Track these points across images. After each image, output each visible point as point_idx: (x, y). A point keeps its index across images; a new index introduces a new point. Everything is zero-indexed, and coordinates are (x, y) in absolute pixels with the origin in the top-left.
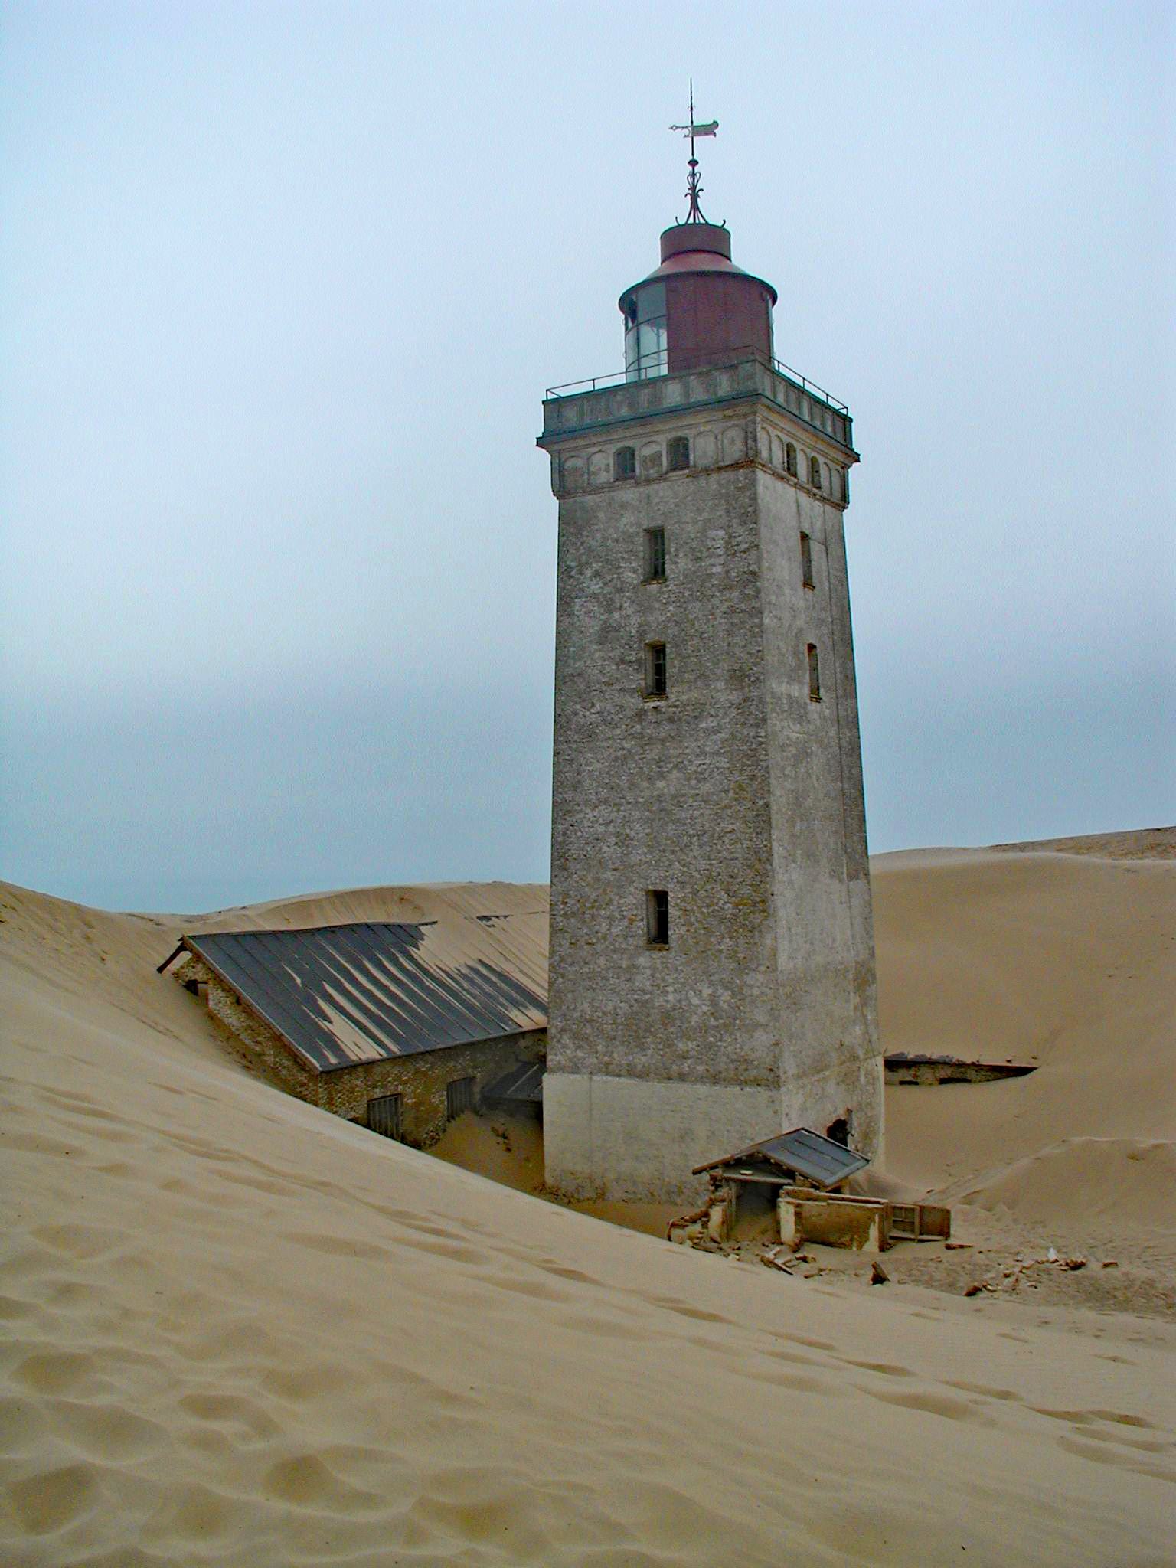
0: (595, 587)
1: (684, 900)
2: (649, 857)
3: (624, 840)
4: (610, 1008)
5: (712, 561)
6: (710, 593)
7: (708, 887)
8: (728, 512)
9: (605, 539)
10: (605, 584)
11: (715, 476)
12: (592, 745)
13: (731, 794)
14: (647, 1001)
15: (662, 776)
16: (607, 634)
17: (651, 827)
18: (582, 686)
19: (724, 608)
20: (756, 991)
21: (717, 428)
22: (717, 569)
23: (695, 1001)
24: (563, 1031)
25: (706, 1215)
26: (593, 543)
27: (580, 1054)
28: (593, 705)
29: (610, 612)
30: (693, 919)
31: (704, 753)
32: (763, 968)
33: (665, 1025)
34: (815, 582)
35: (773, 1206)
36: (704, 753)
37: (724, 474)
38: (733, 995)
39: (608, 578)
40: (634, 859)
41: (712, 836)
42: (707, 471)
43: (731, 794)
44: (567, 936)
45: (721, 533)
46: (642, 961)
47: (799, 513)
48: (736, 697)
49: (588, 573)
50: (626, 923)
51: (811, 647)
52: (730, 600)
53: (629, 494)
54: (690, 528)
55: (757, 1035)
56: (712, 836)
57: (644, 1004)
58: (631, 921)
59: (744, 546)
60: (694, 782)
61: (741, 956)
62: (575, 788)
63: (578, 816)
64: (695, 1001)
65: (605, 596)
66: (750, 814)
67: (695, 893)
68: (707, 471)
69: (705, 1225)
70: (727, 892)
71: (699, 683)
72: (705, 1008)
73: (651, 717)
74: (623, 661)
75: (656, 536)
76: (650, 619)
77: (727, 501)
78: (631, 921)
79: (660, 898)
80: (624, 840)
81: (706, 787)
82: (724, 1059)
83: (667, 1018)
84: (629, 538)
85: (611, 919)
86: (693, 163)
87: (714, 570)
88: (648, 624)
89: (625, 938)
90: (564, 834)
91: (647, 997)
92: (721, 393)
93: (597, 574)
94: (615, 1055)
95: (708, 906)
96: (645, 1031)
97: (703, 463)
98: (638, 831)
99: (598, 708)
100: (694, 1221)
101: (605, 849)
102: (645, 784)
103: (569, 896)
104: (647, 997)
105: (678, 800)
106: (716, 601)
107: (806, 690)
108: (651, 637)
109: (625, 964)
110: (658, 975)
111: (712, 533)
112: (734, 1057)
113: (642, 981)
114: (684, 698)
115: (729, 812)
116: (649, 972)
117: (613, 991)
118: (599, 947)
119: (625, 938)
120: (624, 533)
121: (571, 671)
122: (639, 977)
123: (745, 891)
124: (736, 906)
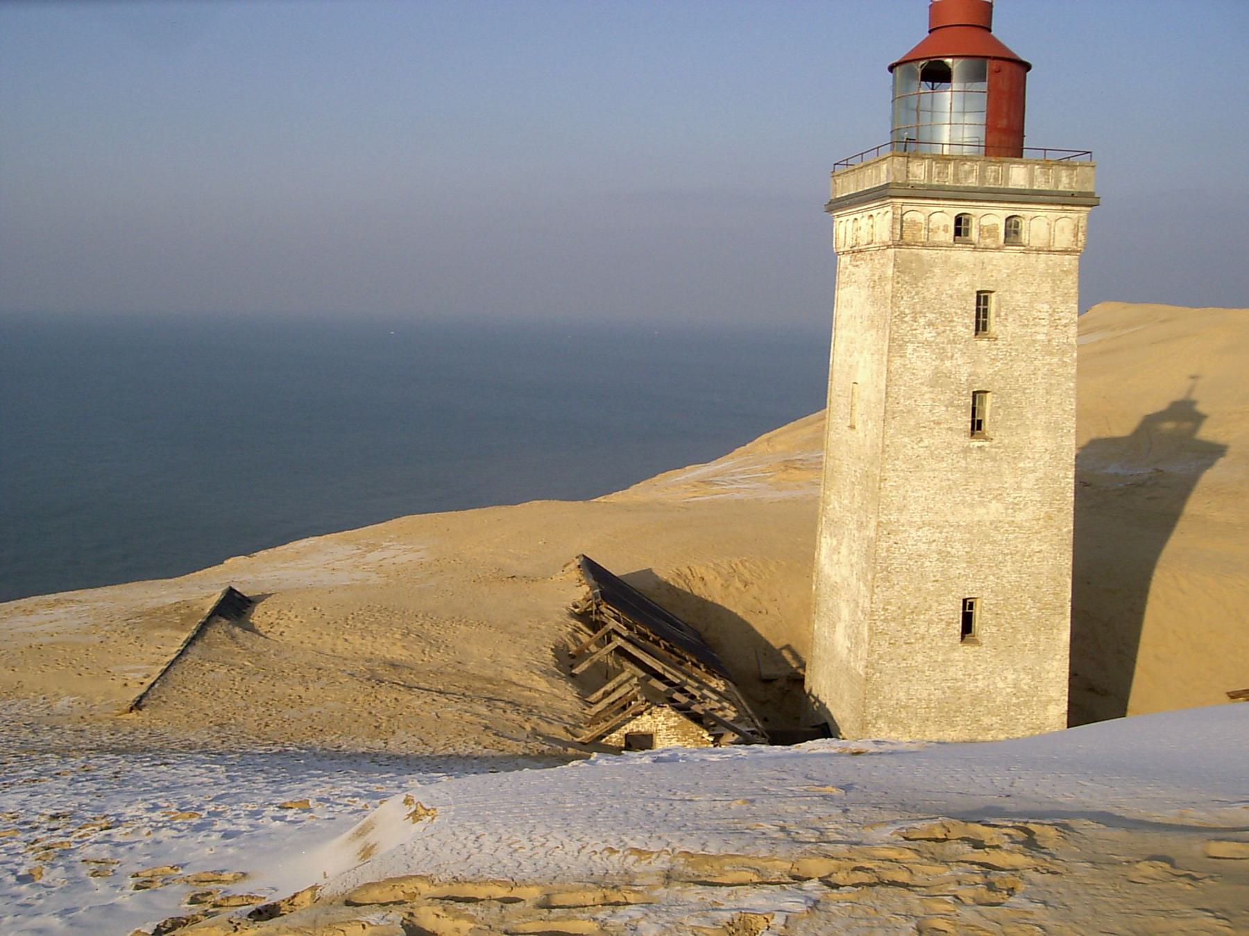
0: (928, 334)
1: (996, 605)
3: (944, 556)
4: (925, 695)
5: (1037, 329)
8: (1054, 291)
9: (939, 293)
10: (938, 334)
11: (1043, 256)
14: (959, 688)
16: (938, 380)
18: (912, 423)
19: (1044, 370)
20: (1051, 675)
22: (1040, 337)
23: (1001, 685)
24: (878, 717)
28: (921, 440)
31: (1020, 488)
36: (1020, 488)
37: (1052, 256)
38: (1033, 679)
41: (1023, 555)
42: (1038, 250)
43: (1041, 522)
44: (887, 638)
45: (1046, 307)
48: (1050, 445)
49: (922, 321)
50: (943, 625)
53: (963, 255)
54: (1018, 297)
55: (1050, 707)
57: (955, 690)
58: (948, 624)
59: (1064, 321)
64: (1001, 685)
65: (937, 344)
68: (1038, 250)
72: (1009, 690)
74: (951, 404)
75: (982, 298)
76: (979, 371)
77: (1054, 281)
78: (948, 624)
80: (944, 556)
81: (1020, 517)
83: (976, 700)
84: (963, 297)
87: (1039, 337)
88: (977, 375)
89: (942, 637)
92: (1061, 188)
93: (930, 324)
95: (1017, 610)
97: (1035, 243)
98: (959, 549)
99: (926, 443)
102: (967, 511)
111: (1038, 306)
114: (1006, 441)
115: (1039, 536)
116: (962, 664)
119: (942, 637)
120: (958, 290)
122: (953, 669)
123: (1049, 598)
124: (1040, 610)
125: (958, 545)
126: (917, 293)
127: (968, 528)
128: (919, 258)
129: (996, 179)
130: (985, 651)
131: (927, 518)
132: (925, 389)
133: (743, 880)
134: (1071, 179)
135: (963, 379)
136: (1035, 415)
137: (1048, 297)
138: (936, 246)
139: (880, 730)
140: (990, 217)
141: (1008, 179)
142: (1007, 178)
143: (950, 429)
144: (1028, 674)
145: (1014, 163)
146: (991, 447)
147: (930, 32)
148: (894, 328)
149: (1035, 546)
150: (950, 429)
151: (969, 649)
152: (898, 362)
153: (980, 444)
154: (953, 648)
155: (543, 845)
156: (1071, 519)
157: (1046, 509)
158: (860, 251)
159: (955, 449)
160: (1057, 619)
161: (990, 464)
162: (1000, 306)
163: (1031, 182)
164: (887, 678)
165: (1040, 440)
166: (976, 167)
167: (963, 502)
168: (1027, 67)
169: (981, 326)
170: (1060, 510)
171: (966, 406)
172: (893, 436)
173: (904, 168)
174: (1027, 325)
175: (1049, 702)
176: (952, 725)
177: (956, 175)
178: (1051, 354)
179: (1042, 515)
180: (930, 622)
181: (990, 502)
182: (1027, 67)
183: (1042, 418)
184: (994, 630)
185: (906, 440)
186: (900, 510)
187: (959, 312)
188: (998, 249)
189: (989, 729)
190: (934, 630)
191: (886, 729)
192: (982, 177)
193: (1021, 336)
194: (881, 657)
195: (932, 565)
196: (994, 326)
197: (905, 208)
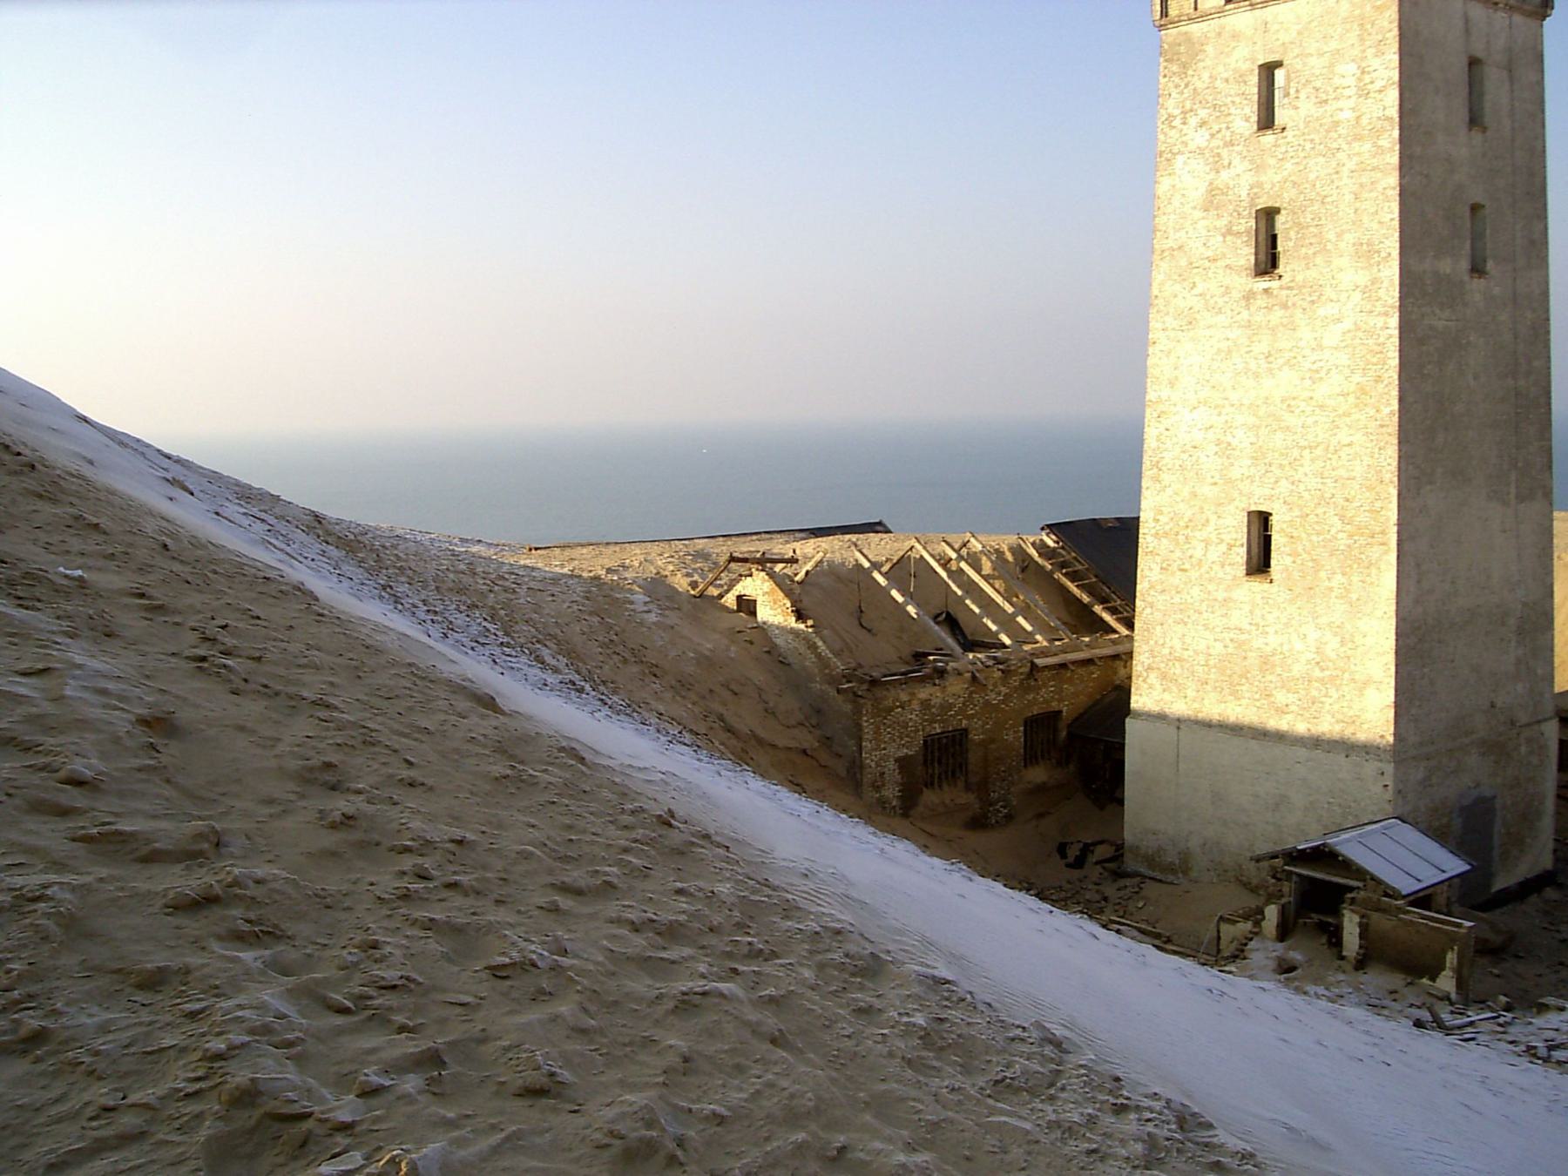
3: (1226, 449)
4: (1202, 646)
5: (1341, 104)
6: (1335, 145)
8: (1362, 40)
10: (1212, 136)
12: (1191, 333)
13: (1351, 399)
14: (1244, 642)
17: (1257, 436)
18: (1183, 262)
19: (1351, 165)
24: (1150, 668)
25: (1260, 911)
26: (1199, 85)
27: (1167, 696)
30: (1300, 549)
31: (1321, 347)
32: (1379, 613)
34: (1488, 119)
35: (1337, 913)
36: (1321, 347)
38: (1343, 643)
39: (1216, 128)
40: (1235, 473)
41: (1327, 449)
43: (1351, 399)
44: (1158, 559)
47: (1467, 31)
48: (1363, 278)
50: (1223, 547)
51: (1475, 208)
56: (1327, 449)
57: (1240, 645)
58: (1230, 547)
59: (1378, 85)
60: (1308, 382)
61: (1354, 596)
62: (1172, 384)
69: (1257, 923)
70: (1342, 518)
71: (1319, 260)
73: (1261, 301)
74: (1229, 232)
76: (1263, 178)
78: (1230, 547)
79: (1261, 523)
80: (1226, 449)
82: (1329, 717)
83: (1266, 663)
84: (1241, 78)
85: (1207, 542)
88: (1260, 185)
91: (1243, 637)
93: (1203, 124)
94: (1206, 702)
96: (1241, 676)
100: (1246, 918)
101: (1203, 459)
104: (1243, 637)
106: (1341, 155)
107: (1465, 265)
108: (1263, 203)
109: (1221, 595)
110: (1258, 612)
112: (1340, 717)
113: (1238, 618)
115: (1348, 420)
116: (1247, 608)
117: (1206, 626)
118: (1194, 574)
120: (1235, 71)
121: (1170, 243)
123: (1363, 518)
124: (1351, 536)
126: (1187, 86)
128: (1188, 38)
136: (1339, 235)
137: (1356, 52)
138: (1205, 17)
144: (1336, 634)
146: (1281, 288)
149: (1343, 436)
151: (1257, 585)
156: (1395, 393)
157: (1357, 378)
160: (1375, 553)
162: (1288, 79)
165: (1350, 275)
170: (1378, 379)
171: (1248, 232)
172: (1162, 284)
174: (1326, 101)
175: (1366, 684)
176: (1235, 694)
179: (1352, 387)
181: (1280, 369)
184: (1288, 560)
185: (1178, 287)
187: (1237, 100)
189: (1282, 711)
193: (1318, 119)
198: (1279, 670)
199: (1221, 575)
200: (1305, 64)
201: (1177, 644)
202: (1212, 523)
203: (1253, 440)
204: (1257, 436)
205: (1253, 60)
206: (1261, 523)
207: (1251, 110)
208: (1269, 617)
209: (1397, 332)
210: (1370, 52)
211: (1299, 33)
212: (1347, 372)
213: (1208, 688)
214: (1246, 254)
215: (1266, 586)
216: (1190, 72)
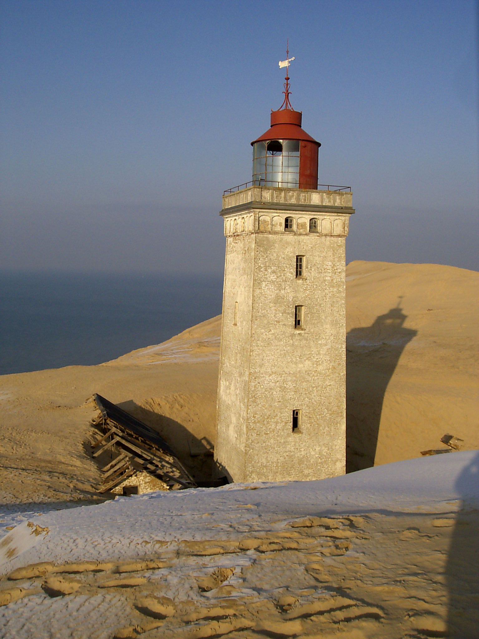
1: (309, 413)
2: (295, 396)
3: (283, 389)
5: (326, 274)
7: (320, 408)
8: (334, 255)
10: (278, 277)
11: (328, 238)
14: (292, 456)
15: (301, 362)
16: (278, 300)
17: (296, 384)
18: (265, 322)
21: (333, 218)
23: (313, 453)
26: (272, 257)
28: (270, 331)
29: (280, 290)
33: (300, 465)
39: (279, 274)
42: (326, 235)
45: (330, 263)
46: (290, 439)
48: (334, 332)
49: (270, 271)
52: (332, 292)
53: (289, 237)
54: (317, 258)
57: (290, 457)
58: (286, 423)
59: (339, 270)
63: (263, 379)
64: (313, 453)
65: (277, 282)
66: (337, 379)
67: (314, 410)
68: (326, 235)
72: (317, 456)
74: (284, 312)
75: (299, 259)
76: (298, 295)
77: (333, 250)
78: (286, 423)
79: (295, 414)
80: (283, 389)
81: (320, 368)
83: (301, 462)
84: (290, 259)
86: (287, 79)
89: (283, 430)
90: (255, 386)
91: (292, 454)
92: (336, 205)
93: (274, 272)
95: (320, 415)
97: (324, 232)
102: (294, 366)
103: (256, 414)
104: (292, 454)
105: (308, 373)
111: (327, 263)
116: (293, 443)
117: (277, 453)
120: (287, 255)
123: (335, 408)
124: (331, 415)
125: (290, 383)
126: (267, 257)
127: (294, 374)
129: (305, 200)
130: (305, 436)
131: (274, 370)
132: (272, 305)
133: (216, 552)
134: (341, 200)
135: (291, 300)
136: (326, 317)
137: (331, 258)
138: (276, 233)
139: (253, 479)
140: (302, 219)
141: (311, 200)
142: (310, 200)
143: (284, 325)
145: (314, 192)
146: (305, 333)
147: (271, 126)
148: (256, 274)
149: (327, 383)
150: (284, 325)
151: (296, 436)
152: (258, 291)
153: (300, 332)
154: (288, 436)
155: (110, 542)
156: (345, 368)
157: (333, 363)
158: (238, 235)
159: (287, 335)
160: (339, 419)
161: (304, 342)
162: (307, 263)
163: (322, 202)
164: (256, 452)
165: (328, 329)
166: (295, 194)
167: (292, 362)
168: (319, 145)
169: (299, 273)
172: (256, 329)
173: (260, 194)
175: (337, 461)
176: (289, 474)
177: (285, 197)
178: (333, 287)
180: (277, 423)
181: (305, 361)
182: (319, 145)
183: (329, 318)
184: (309, 425)
185: (263, 331)
186: (261, 366)
188: (306, 234)
190: (279, 426)
191: (256, 478)
192: (298, 199)
194: (252, 441)
195: (276, 394)
196: (305, 273)
197: (261, 214)
198: (305, 463)
199: (282, 434)
200: (313, 259)
201: (264, 461)
202: (279, 415)
203: (294, 385)
204: (296, 384)
205: (294, 253)
206: (295, 414)
207: (294, 271)
208: (302, 446)
209: (345, 350)
210: (336, 259)
211: (312, 248)
212: (329, 362)
213: (278, 474)
214: (292, 321)
215: (300, 435)
216: (268, 252)
